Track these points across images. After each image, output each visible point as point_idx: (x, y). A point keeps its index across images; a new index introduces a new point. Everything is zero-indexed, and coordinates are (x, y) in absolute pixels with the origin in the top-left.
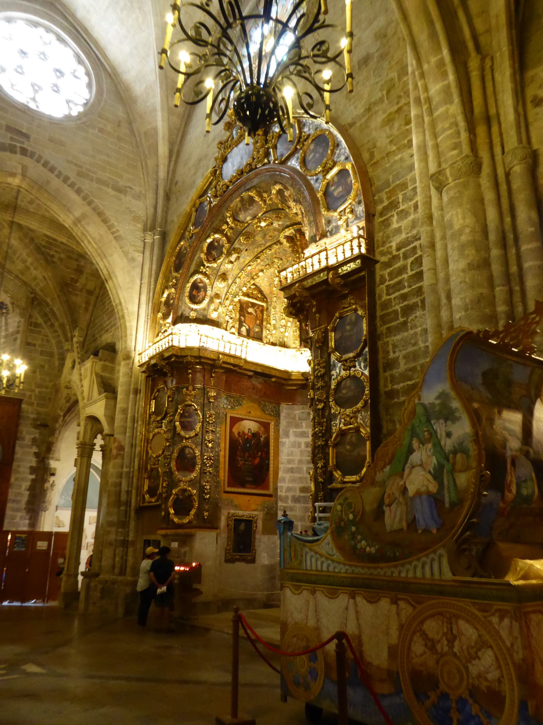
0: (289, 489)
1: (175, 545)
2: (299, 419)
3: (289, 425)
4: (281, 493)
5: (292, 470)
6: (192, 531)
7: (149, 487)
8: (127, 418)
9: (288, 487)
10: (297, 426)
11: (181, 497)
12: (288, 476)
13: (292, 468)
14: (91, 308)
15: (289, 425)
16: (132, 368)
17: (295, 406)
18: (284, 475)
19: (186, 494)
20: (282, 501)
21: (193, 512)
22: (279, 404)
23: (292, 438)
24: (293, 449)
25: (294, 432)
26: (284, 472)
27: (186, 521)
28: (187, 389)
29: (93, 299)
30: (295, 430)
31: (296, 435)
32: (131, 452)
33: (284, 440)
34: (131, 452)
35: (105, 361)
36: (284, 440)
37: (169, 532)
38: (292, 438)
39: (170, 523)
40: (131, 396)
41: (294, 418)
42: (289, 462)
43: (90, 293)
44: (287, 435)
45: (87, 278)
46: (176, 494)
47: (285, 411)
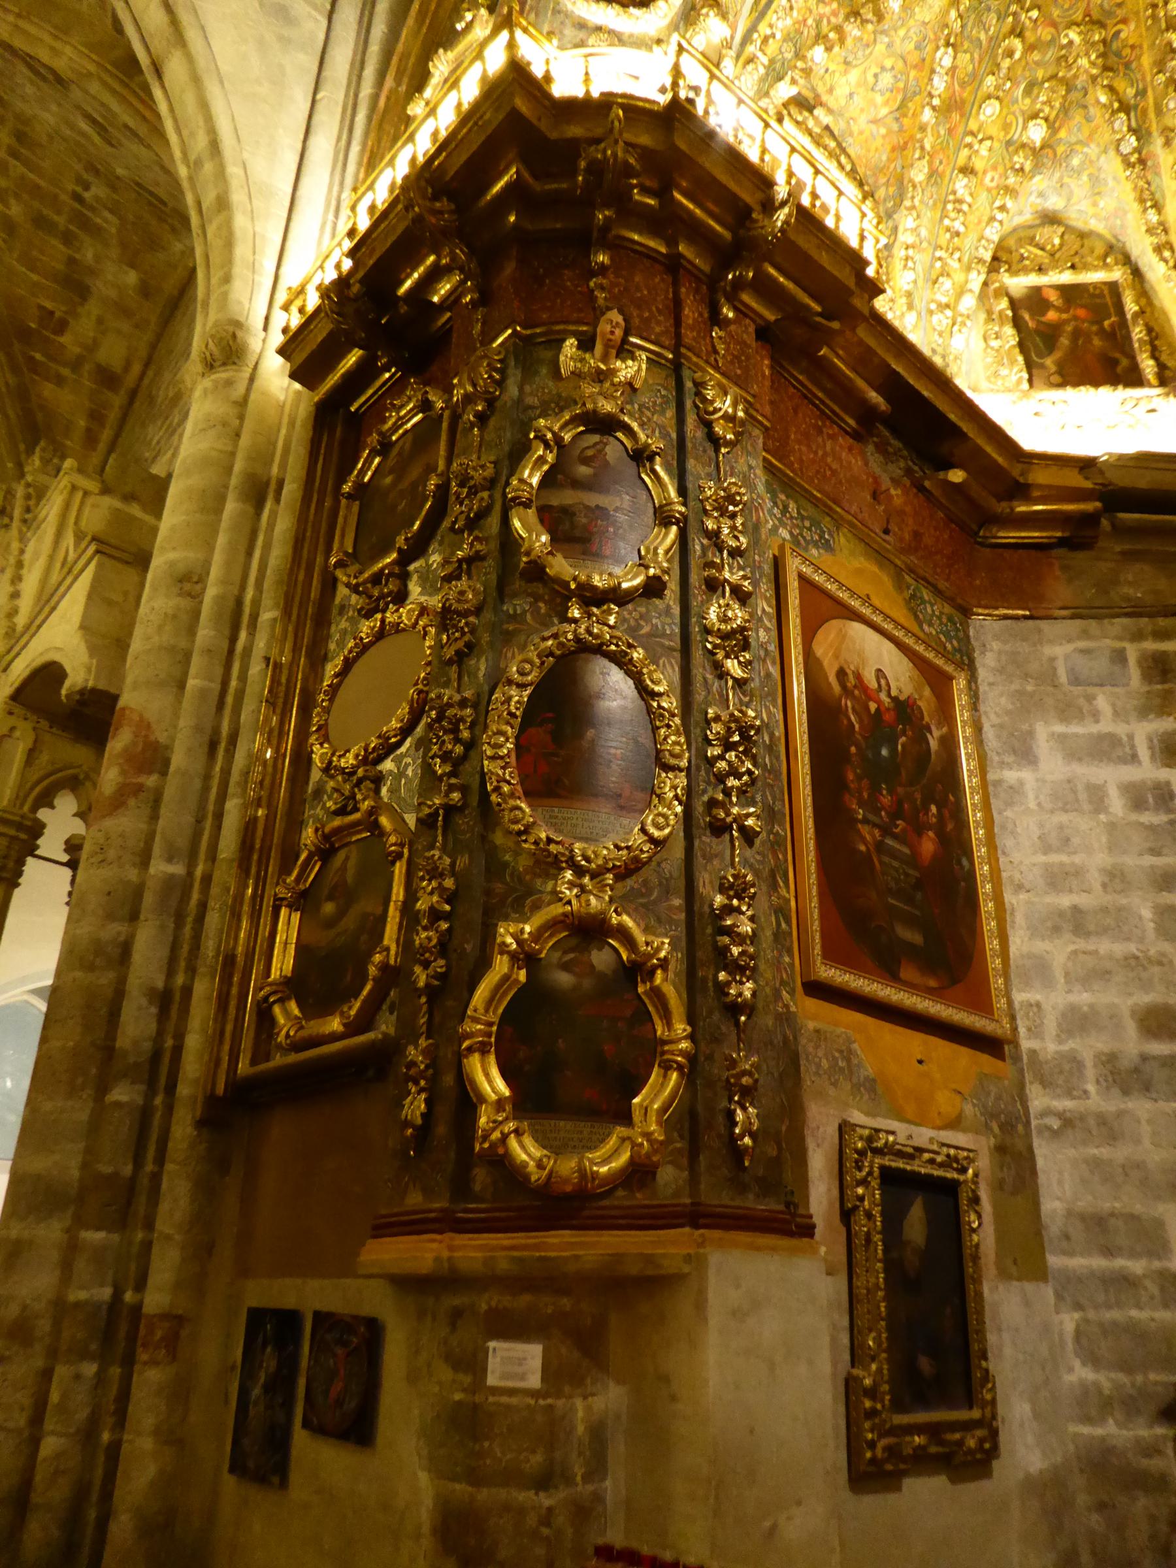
0: (1078, 1021)
1: (516, 1364)
2: (1076, 681)
3: (1027, 705)
4: (1040, 1041)
5: (1076, 922)
6: (670, 1246)
7: (303, 951)
8: (196, 614)
9: (1073, 1009)
10: (1067, 711)
11: (564, 979)
12: (1059, 952)
13: (1075, 909)
14: (106, 435)
15: (1027, 705)
16: (243, 403)
17: (1044, 625)
18: (1041, 946)
19: (600, 959)
20: (1045, 1083)
21: (656, 1095)
22: (966, 613)
23: (1052, 766)
24: (1064, 818)
25: (1062, 738)
26: (1034, 932)
27: (607, 1159)
28: (586, 344)
29: (117, 401)
30: (1059, 728)
31: (1072, 751)
32: (207, 777)
33: (1011, 776)
34: (207, 777)
35: (129, 498)
36: (1011, 776)
37: (472, 1250)
38: (1052, 766)
39: (480, 1177)
40: (231, 506)
41: (1048, 677)
42: (1056, 879)
43: (108, 378)
44: (1025, 754)
45: (100, 321)
46: (526, 957)
47: (996, 645)
